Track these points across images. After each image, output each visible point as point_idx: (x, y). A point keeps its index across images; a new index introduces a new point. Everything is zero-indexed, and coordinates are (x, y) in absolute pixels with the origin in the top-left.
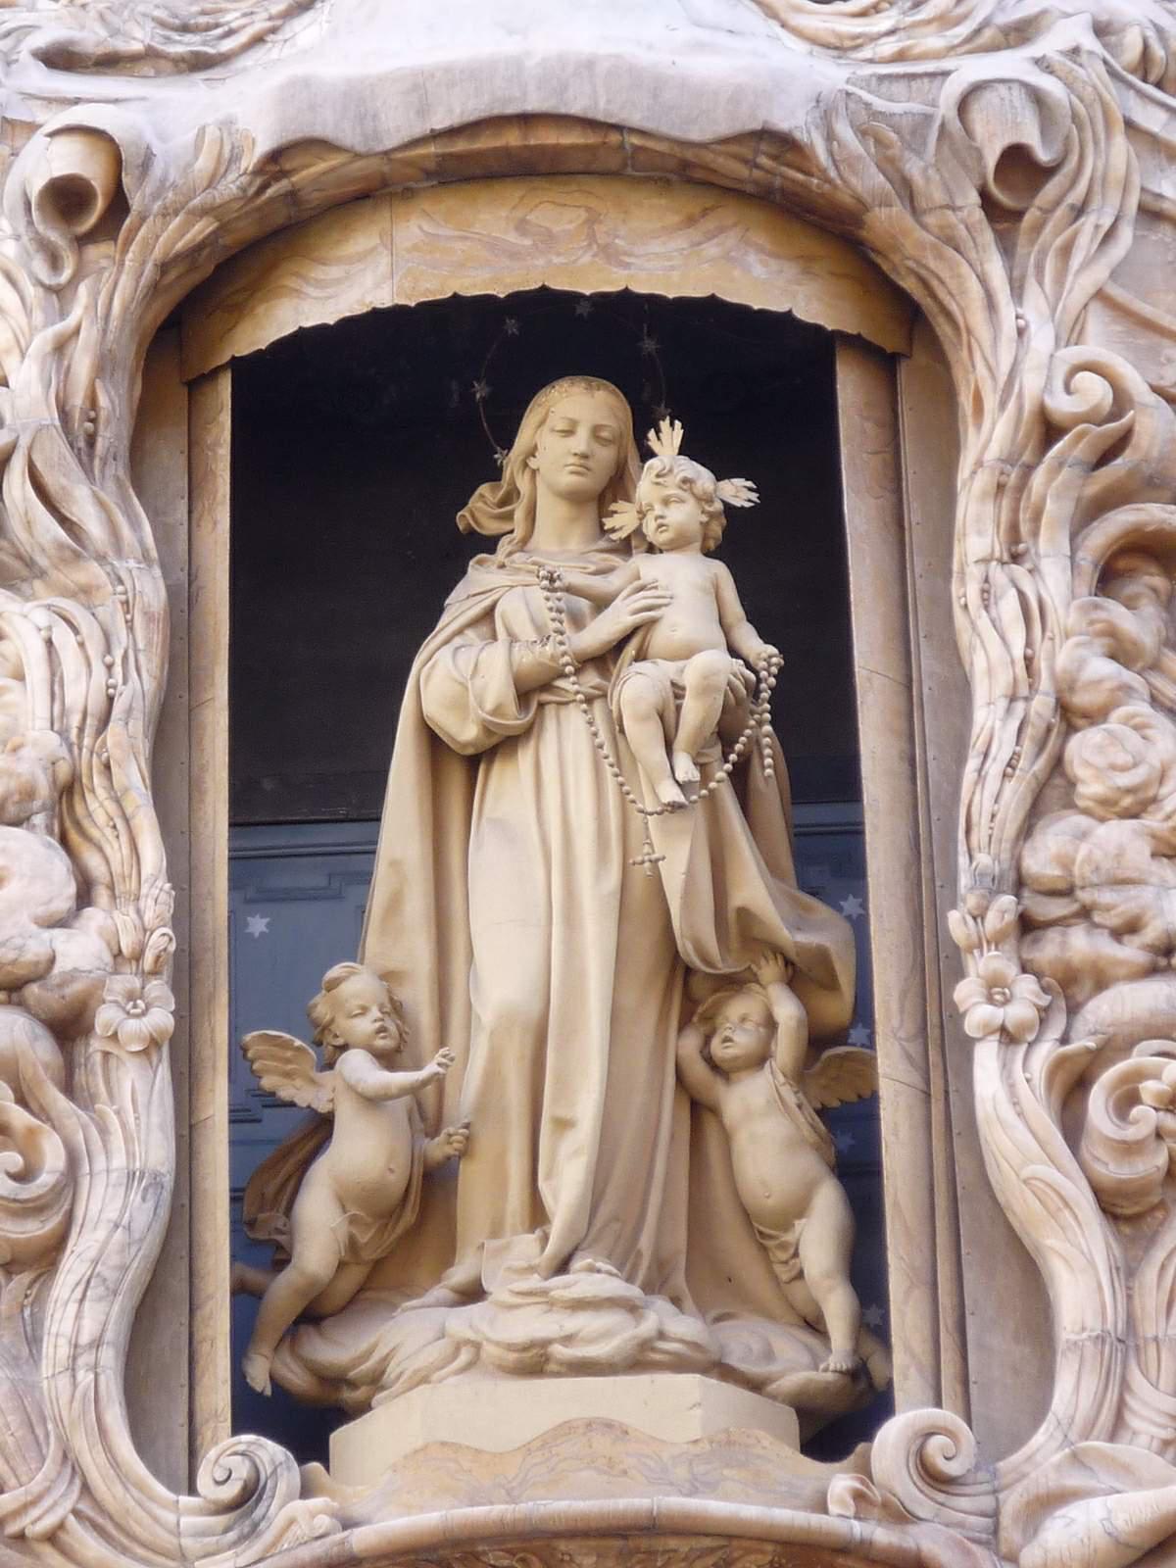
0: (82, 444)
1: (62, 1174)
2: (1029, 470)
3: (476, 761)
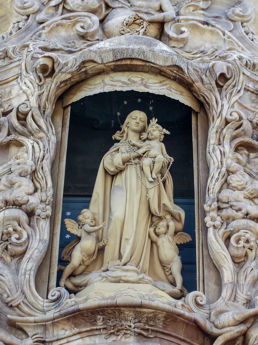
0: (42, 112)
1: (26, 239)
2: (223, 129)
3: (114, 176)
